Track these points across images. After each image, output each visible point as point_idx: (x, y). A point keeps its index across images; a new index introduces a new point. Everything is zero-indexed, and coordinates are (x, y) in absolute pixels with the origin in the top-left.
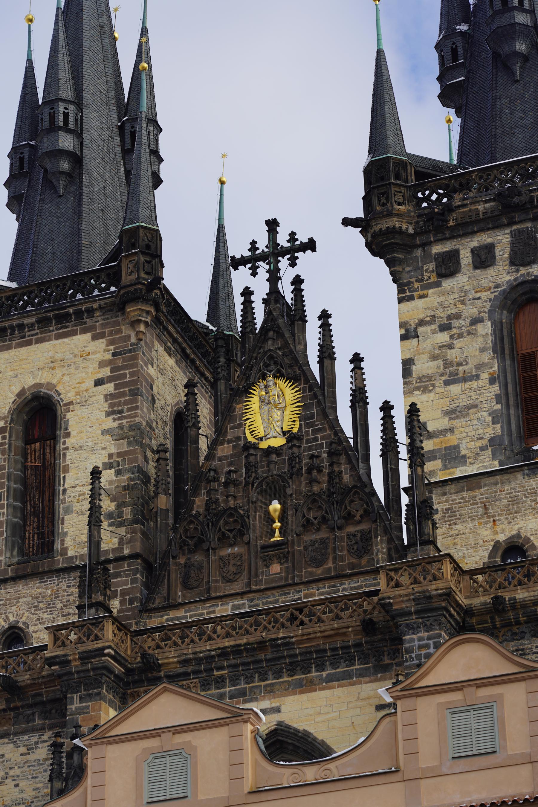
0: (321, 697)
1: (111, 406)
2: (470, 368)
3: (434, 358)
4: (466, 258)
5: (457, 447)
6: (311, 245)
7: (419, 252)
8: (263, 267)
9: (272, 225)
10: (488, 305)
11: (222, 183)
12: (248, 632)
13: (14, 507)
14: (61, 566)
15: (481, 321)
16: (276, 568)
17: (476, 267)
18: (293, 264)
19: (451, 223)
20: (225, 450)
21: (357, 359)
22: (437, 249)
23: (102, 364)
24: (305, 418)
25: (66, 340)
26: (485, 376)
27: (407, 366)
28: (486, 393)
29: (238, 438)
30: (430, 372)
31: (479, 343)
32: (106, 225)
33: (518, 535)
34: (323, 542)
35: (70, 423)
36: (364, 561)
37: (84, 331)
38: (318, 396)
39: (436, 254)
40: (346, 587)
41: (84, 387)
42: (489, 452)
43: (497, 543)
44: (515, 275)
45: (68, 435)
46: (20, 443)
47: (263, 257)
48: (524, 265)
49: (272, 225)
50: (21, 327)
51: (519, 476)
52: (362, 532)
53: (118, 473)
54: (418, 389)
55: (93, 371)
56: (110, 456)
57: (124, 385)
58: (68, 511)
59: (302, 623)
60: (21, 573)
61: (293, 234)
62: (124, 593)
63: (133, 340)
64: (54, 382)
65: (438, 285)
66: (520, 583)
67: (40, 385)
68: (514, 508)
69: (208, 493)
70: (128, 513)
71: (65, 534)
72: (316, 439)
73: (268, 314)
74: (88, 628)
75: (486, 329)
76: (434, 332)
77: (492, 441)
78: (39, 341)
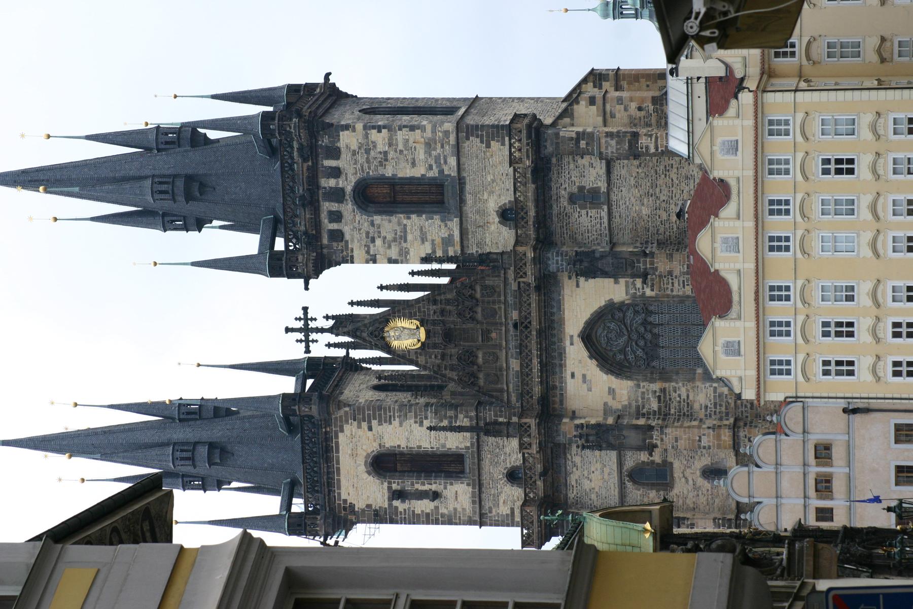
0: (568, 315)
1: (386, 422)
2: (398, 229)
3: (389, 247)
4: (334, 226)
5: (443, 239)
6: (305, 309)
7: (325, 251)
8: (313, 336)
9: (288, 330)
10: (364, 217)
11: (199, 365)
12: (530, 351)
13: (436, 477)
14: (475, 450)
15: (372, 221)
16: (494, 335)
17: (341, 221)
18: (315, 319)
19: (314, 232)
20: (422, 360)
21: (381, 288)
22: (325, 241)
23: (359, 427)
24: (410, 317)
25: (340, 448)
26: (405, 222)
27: (391, 261)
28: (414, 222)
29: (416, 353)
30: (397, 250)
31: (386, 223)
32: (256, 428)
33: (497, 212)
34: (483, 310)
35: (392, 444)
36: (498, 290)
37: (337, 437)
38: (397, 309)
39: (329, 241)
40: (510, 300)
41: (371, 438)
42: (449, 223)
43: (499, 222)
44: (349, 201)
45: (399, 446)
46: (397, 474)
47: (307, 336)
48: (344, 196)
49: (288, 330)
50: (328, 473)
51: (465, 208)
52: (482, 290)
53: (426, 418)
54: (406, 257)
55: (363, 432)
56: (416, 422)
57: (374, 414)
58: (444, 446)
59: (530, 323)
60: (477, 472)
61: (296, 319)
62: (496, 415)
63: (347, 409)
64: (365, 454)
65: (347, 242)
66: (526, 213)
67: (366, 462)
68: (482, 212)
69: (446, 369)
70: (450, 413)
71: (457, 447)
72: (424, 312)
73: (344, 334)
74: (522, 431)
75: (377, 219)
76: (375, 246)
77: (442, 221)
78: (338, 463)
